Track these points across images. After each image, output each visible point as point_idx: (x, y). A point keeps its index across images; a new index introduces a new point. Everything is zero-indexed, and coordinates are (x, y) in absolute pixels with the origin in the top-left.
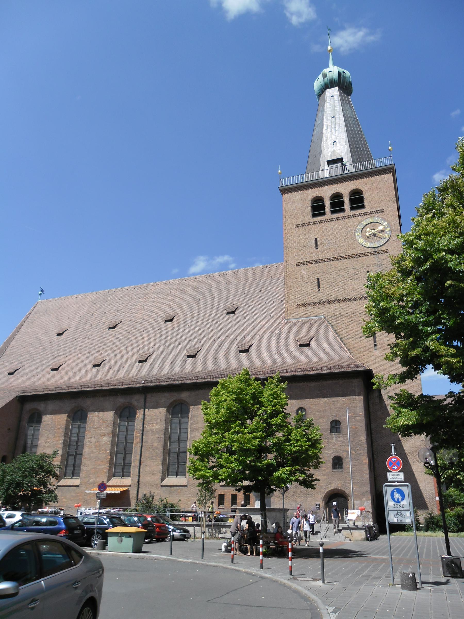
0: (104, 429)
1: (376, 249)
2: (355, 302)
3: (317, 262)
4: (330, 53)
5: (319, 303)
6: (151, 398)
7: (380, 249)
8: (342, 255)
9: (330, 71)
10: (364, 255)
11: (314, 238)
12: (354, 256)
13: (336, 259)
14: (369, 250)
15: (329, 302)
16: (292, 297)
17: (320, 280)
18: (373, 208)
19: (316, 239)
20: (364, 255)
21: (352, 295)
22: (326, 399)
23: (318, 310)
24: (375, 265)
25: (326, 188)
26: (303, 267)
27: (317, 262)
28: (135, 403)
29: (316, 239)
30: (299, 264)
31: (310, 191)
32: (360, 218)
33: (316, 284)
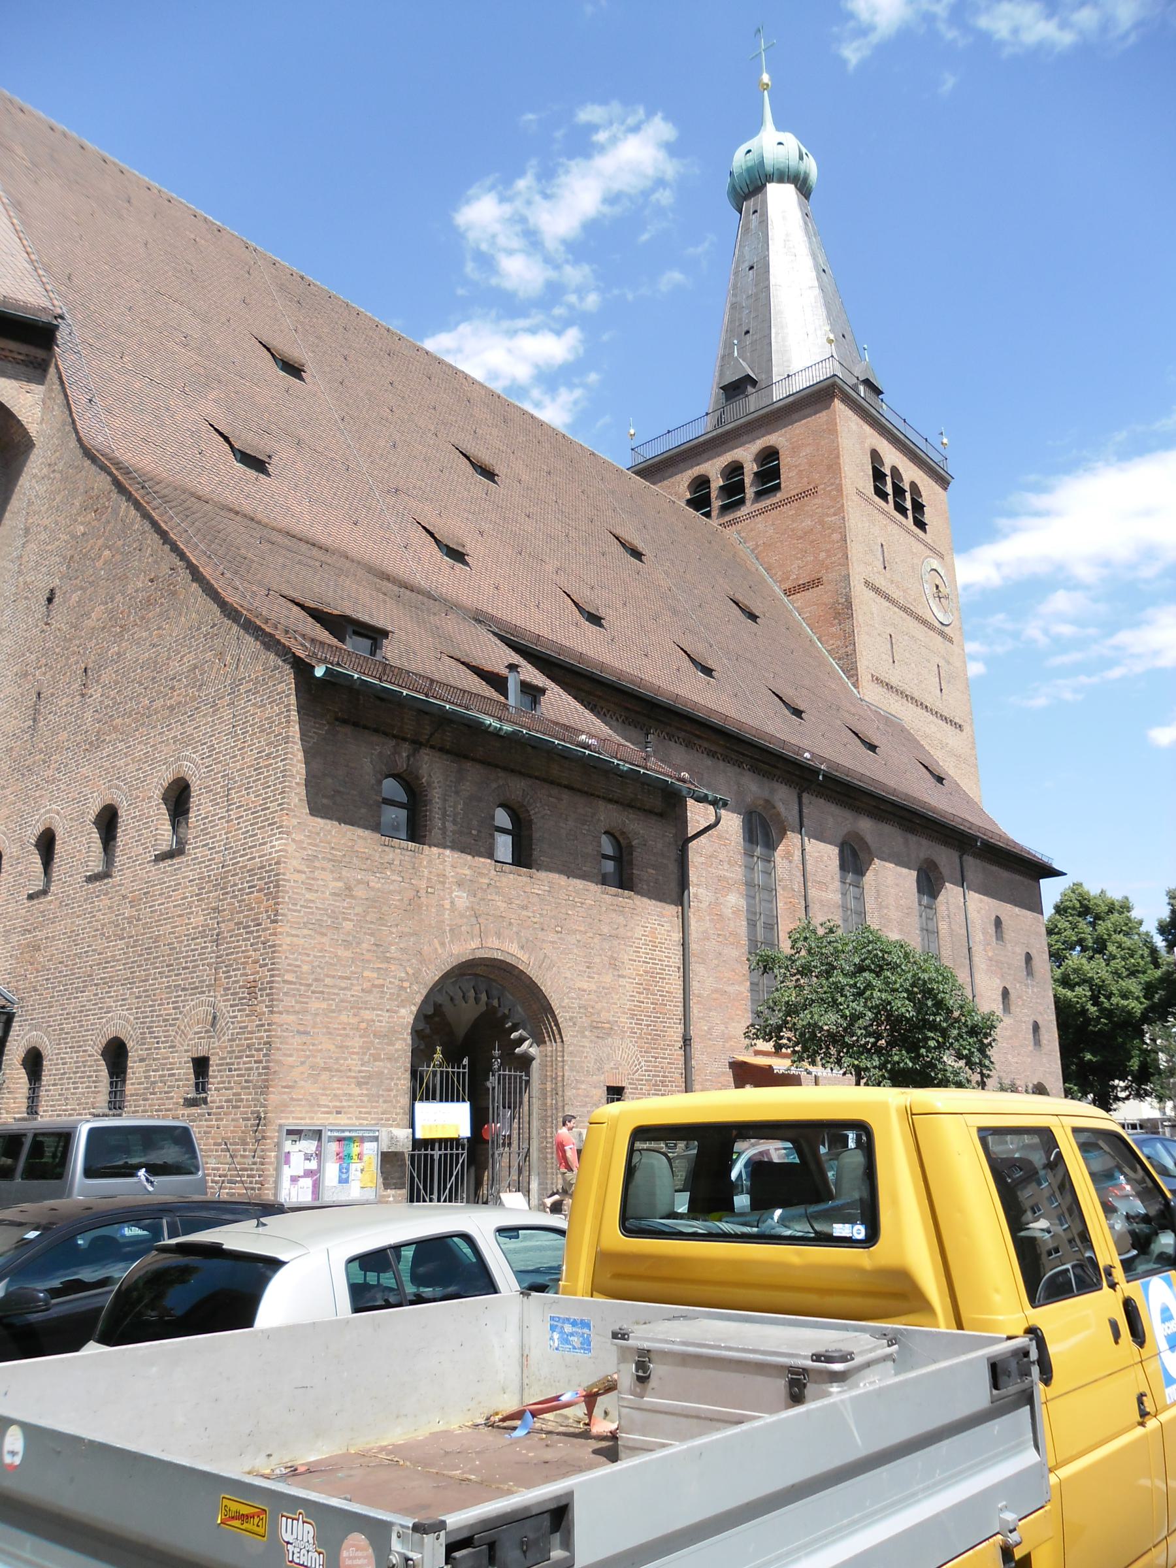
0: (726, 866)
1: (943, 628)
3: (887, 597)
4: (766, 92)
6: (818, 809)
7: (946, 630)
8: (913, 609)
10: (931, 627)
13: (905, 609)
14: (937, 624)
16: (864, 653)
18: (934, 541)
22: (1017, 909)
26: (872, 594)
27: (887, 597)
28: (781, 808)
30: (867, 583)
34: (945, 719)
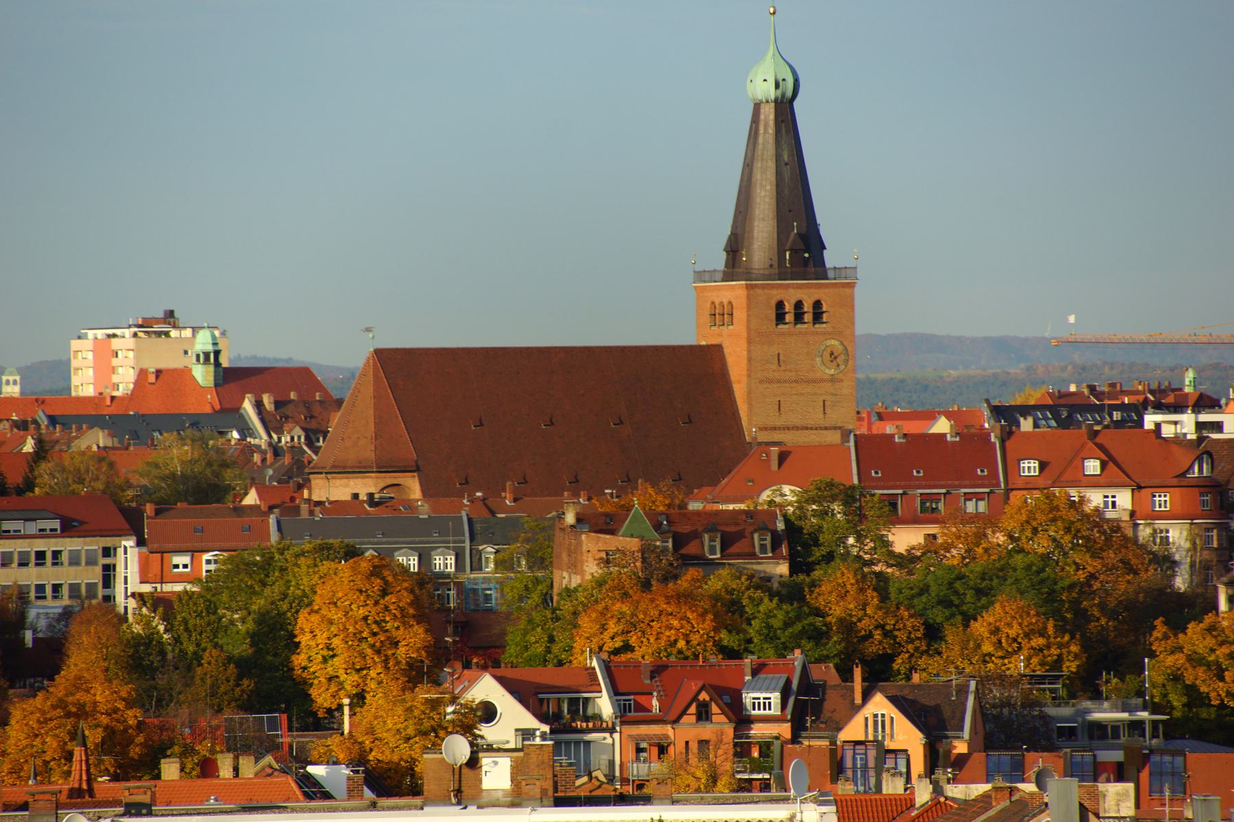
2: (811, 432)
5: (779, 429)
9: (784, 80)
11: (777, 352)
12: (814, 381)
14: (827, 377)
15: (788, 429)
17: (781, 403)
19: (779, 354)
20: (822, 381)
21: (811, 423)
23: (779, 436)
24: (832, 394)
25: (792, 291)
27: (779, 381)
29: (779, 354)
31: (774, 292)
32: (820, 337)
33: (777, 407)
34: (826, 428)
